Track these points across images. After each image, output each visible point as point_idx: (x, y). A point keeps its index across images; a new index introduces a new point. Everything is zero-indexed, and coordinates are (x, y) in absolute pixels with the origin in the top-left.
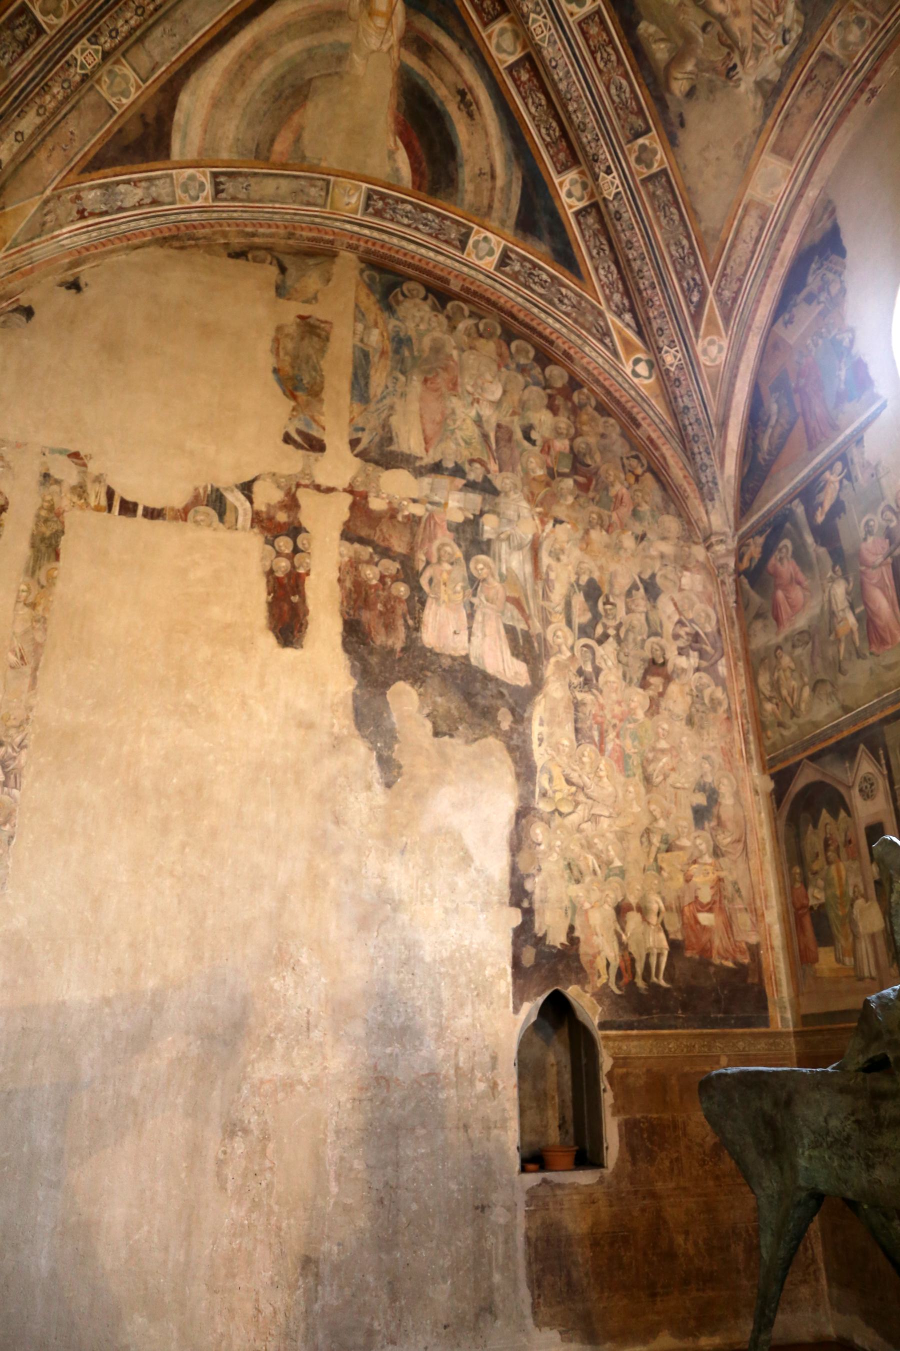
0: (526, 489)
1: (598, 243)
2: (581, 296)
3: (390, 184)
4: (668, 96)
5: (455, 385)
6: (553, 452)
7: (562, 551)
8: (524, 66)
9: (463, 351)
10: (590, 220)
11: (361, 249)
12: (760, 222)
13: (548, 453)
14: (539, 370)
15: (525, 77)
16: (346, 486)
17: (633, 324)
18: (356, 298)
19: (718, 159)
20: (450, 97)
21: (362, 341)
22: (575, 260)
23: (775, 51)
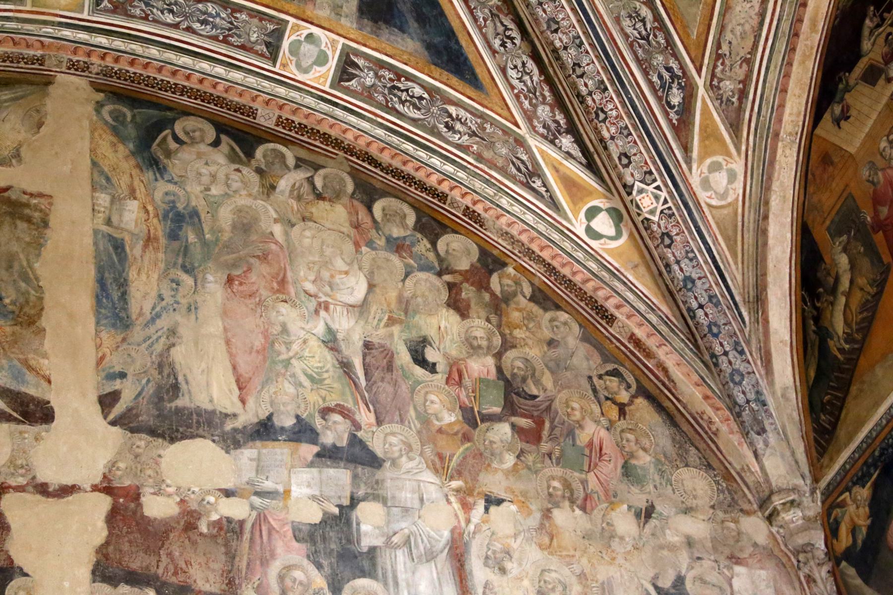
0: (428, 450)
1: (501, 29)
2: (482, 116)
5: (283, 282)
6: (467, 381)
7: (508, 553)
9: (293, 225)
11: (95, 69)
13: (460, 383)
14: (425, 244)
16: (98, 480)
17: (576, 152)
18: (93, 151)
21: (109, 222)
22: (466, 59)
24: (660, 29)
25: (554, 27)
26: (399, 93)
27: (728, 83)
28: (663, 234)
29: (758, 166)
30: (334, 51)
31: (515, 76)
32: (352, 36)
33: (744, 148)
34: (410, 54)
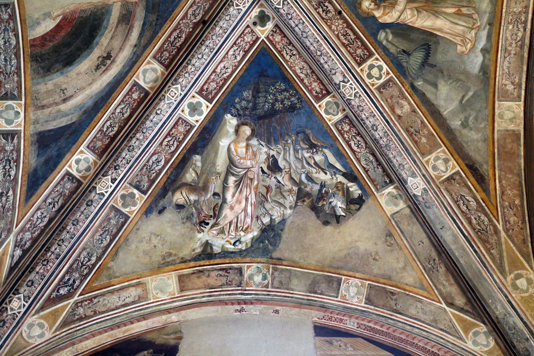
1: (56, 200)
3: (25, 20)
4: (170, 193)
8: (141, 93)
10: (69, 185)
12: (137, 299)
15: (135, 96)
17: (15, 259)
19: (155, 246)
20: (103, 49)
22: (37, 190)
23: (227, 241)
24: (89, 269)
25: (75, 223)
26: (8, 164)
27: (82, 310)
28: (4, 320)
29: (54, 344)
30: (15, 127)
31: (38, 215)
32: (26, 133)
33: (58, 333)
34: (29, 163)
